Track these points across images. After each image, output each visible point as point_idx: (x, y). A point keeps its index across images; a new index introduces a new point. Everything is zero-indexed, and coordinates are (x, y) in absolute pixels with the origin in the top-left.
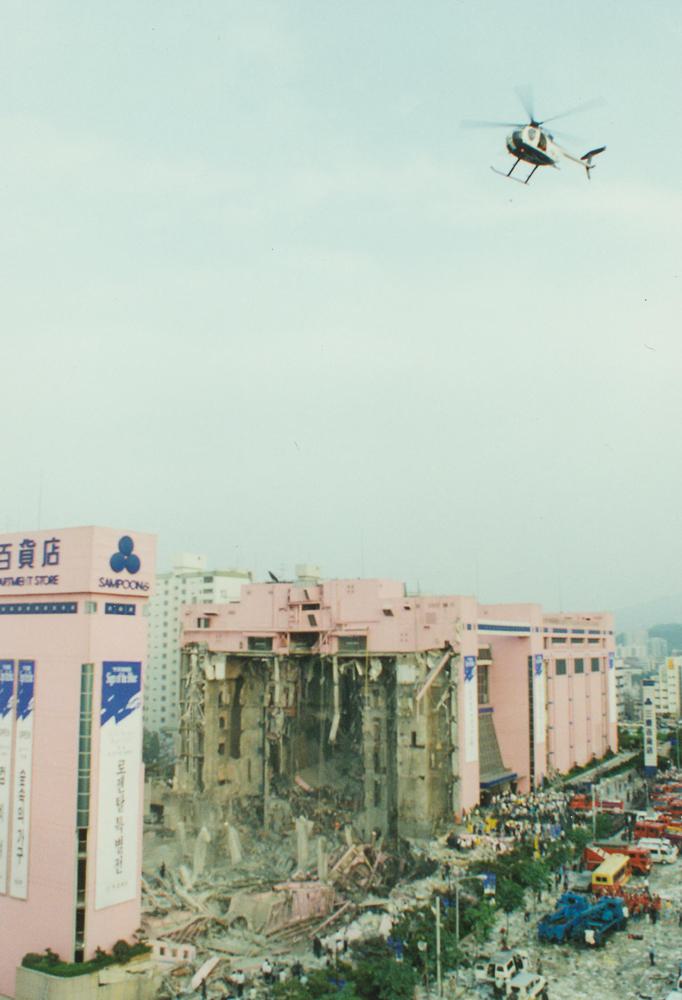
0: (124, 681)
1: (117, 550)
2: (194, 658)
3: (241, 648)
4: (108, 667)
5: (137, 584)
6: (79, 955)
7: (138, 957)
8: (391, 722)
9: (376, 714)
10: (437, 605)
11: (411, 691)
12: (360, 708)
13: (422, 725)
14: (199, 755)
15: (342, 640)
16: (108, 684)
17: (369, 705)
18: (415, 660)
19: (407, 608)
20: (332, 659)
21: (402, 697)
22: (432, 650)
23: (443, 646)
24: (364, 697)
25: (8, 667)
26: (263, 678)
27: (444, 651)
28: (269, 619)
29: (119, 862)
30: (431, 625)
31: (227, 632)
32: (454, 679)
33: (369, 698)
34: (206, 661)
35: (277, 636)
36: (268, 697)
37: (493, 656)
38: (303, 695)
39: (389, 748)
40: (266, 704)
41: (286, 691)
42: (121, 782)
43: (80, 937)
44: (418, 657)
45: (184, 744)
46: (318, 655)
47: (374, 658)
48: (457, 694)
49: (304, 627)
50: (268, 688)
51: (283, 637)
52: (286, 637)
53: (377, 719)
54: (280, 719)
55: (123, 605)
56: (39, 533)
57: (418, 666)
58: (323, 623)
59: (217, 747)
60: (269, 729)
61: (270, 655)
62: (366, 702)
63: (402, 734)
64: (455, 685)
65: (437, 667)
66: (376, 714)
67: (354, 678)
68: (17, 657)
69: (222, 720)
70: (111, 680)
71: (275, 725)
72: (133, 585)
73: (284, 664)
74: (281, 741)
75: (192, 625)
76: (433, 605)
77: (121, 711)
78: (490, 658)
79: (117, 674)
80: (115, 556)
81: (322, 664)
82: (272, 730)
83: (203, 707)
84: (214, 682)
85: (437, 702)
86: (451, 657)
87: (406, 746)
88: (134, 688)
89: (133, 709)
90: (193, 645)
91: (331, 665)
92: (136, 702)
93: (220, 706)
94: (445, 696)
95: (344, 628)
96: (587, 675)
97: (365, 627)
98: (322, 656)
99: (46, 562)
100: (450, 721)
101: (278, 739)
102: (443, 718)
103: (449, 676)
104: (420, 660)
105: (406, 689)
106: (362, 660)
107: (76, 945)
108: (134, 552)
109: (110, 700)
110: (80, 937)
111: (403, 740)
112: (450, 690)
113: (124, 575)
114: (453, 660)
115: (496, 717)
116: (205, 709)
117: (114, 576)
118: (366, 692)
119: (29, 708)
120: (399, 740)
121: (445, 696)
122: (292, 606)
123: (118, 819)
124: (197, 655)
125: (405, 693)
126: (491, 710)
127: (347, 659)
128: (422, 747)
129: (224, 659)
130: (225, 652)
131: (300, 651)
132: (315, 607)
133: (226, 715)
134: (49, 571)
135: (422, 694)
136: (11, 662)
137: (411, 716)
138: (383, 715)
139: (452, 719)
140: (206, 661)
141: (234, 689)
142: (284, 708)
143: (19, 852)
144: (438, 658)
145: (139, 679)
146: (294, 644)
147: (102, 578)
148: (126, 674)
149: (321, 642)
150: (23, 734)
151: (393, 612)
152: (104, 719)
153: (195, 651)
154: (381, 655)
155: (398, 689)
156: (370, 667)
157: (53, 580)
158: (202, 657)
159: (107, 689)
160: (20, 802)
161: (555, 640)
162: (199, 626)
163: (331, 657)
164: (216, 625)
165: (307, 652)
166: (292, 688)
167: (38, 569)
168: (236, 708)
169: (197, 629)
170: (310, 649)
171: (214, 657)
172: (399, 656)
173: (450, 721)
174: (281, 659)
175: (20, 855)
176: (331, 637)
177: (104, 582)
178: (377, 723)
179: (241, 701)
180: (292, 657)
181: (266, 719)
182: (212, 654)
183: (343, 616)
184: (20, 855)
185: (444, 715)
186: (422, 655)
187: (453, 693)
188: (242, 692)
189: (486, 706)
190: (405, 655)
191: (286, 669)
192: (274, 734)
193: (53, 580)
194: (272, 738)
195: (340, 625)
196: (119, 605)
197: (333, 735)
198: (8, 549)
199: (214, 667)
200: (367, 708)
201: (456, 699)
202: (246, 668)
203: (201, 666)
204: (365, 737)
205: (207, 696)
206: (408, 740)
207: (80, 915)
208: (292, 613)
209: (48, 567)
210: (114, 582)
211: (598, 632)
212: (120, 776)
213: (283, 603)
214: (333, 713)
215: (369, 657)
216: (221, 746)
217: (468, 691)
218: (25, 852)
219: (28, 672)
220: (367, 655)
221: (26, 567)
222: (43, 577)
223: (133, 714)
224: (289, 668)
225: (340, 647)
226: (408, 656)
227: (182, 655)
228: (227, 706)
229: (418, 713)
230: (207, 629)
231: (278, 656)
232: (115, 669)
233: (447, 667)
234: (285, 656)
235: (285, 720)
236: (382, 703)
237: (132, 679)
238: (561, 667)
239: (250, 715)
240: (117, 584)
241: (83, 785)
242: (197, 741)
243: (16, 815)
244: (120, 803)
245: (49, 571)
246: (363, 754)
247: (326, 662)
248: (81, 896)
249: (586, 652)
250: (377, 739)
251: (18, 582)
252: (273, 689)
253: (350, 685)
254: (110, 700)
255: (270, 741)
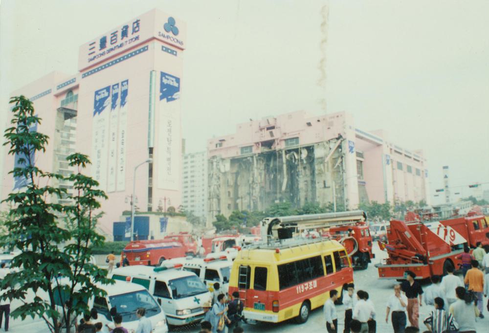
0: (171, 83)
1: (167, 22)
2: (215, 164)
3: (237, 153)
4: (163, 75)
5: (177, 41)
6: (150, 209)
7: (180, 217)
8: (313, 182)
9: (306, 179)
10: (334, 117)
11: (322, 160)
12: (297, 177)
13: (329, 177)
14: (218, 209)
15: (285, 140)
16: (163, 83)
17: (302, 175)
18: (324, 145)
19: (319, 121)
20: (282, 152)
21: (318, 164)
22: (332, 139)
23: (337, 136)
24: (299, 171)
25: (116, 87)
26: (249, 170)
27: (338, 139)
28: (252, 137)
29: (169, 169)
30: (331, 128)
31: (230, 147)
32: (344, 151)
33: (301, 171)
34: (221, 163)
35: (255, 145)
36: (251, 179)
37: (365, 155)
38: (270, 189)
39: (312, 194)
40: (250, 182)
41: (260, 174)
42: (170, 131)
43: (150, 201)
44: (325, 143)
45: (211, 205)
46: (275, 150)
47: (303, 148)
48: (345, 158)
49: (267, 137)
50: (251, 175)
51: (258, 145)
52: (259, 145)
53: (306, 181)
54: (257, 189)
55: (171, 50)
56: (129, 20)
57: (325, 148)
58: (277, 134)
59: (227, 205)
60: (252, 194)
61: (252, 155)
62: (300, 173)
63: (318, 183)
64: (344, 154)
65: (334, 146)
66: (306, 179)
67: (294, 162)
68: (120, 82)
69: (229, 192)
70: (165, 81)
71: (255, 192)
72: (176, 41)
73: (259, 161)
74: (258, 200)
75: (213, 147)
76: (332, 118)
77: (170, 97)
78: (363, 157)
79: (168, 79)
80: (166, 24)
81: (277, 153)
82: (254, 195)
83: (220, 186)
84: (225, 173)
85: (335, 164)
86: (342, 141)
87: (321, 188)
88: (177, 89)
89: (176, 99)
90: (214, 157)
91: (282, 154)
92: (178, 96)
93: (228, 186)
94: (339, 160)
95: (287, 135)
96: (414, 175)
97: (298, 133)
98: (277, 150)
99: (134, 31)
100: (343, 173)
101: (257, 198)
102: (339, 170)
103: (341, 151)
104: (326, 145)
105: (320, 160)
106: (297, 151)
107: (148, 205)
108: (176, 25)
109: (164, 90)
110: (150, 201)
111: (319, 186)
112: (342, 157)
113: (171, 34)
114: (343, 142)
115: (368, 188)
116: (221, 186)
117: (166, 34)
118: (300, 168)
119: (126, 101)
120: (317, 185)
121: (339, 160)
122: (261, 130)
123: (168, 148)
124: (216, 162)
125: (319, 162)
126: (364, 183)
127: (289, 151)
128: (329, 187)
129: (229, 161)
130: (229, 158)
131: (266, 150)
132: (273, 128)
133: (231, 190)
134: (135, 35)
135: (327, 159)
136: (118, 84)
137: (323, 173)
138: (309, 179)
139: (343, 171)
140: (221, 163)
141: (234, 179)
142: (259, 183)
143: (121, 169)
144: (335, 143)
145: (179, 85)
146: (263, 147)
147: (160, 32)
148: (172, 81)
149: (276, 143)
150: (123, 114)
151: (312, 123)
152: (162, 98)
153: (215, 160)
154: (306, 146)
155: (315, 161)
156: (301, 153)
157: (137, 38)
158: (218, 163)
159: (163, 85)
160: (122, 146)
161: (396, 151)
162: (217, 146)
163: (281, 150)
164: (225, 145)
165: (270, 150)
166: (263, 172)
167: (130, 35)
168: (236, 186)
169: (216, 149)
170: (270, 148)
171: (224, 161)
172: (315, 145)
173: (343, 173)
174: (257, 155)
175: (122, 170)
176: (281, 140)
177: (161, 34)
178: (306, 183)
179: (239, 183)
180: (261, 155)
181: (251, 190)
182: (223, 159)
183: (286, 129)
184: (122, 170)
185: (340, 172)
186: (327, 143)
187: (343, 158)
188: (239, 179)
189: (360, 180)
190: (318, 143)
191: (260, 164)
192: (255, 196)
193: (137, 38)
194: (254, 198)
195: (285, 134)
196: (168, 49)
197: (284, 188)
198: (116, 34)
199: (225, 166)
200: (301, 176)
201: (345, 161)
202: (240, 166)
203: (218, 167)
204: (300, 191)
205: (221, 180)
206: (322, 185)
207: (150, 190)
208: (261, 132)
209: (134, 33)
210: (166, 36)
211: (419, 157)
212: (169, 128)
213: (257, 129)
214: (283, 178)
215: (301, 148)
216: (229, 205)
217: (351, 160)
218: (124, 169)
219: (125, 85)
220: (299, 147)
221: (125, 38)
222: (132, 39)
223: (176, 100)
224: (261, 163)
225: (287, 144)
226: (320, 144)
227: (209, 163)
228: (232, 186)
229: (326, 171)
230: (221, 148)
231: (255, 154)
232: (167, 77)
233: (340, 147)
234: (259, 154)
235: (260, 190)
236: (308, 172)
237: (176, 85)
238: (400, 166)
239: (243, 191)
240: (168, 37)
241: (150, 99)
242: (217, 204)
243: (120, 151)
244: (169, 141)
245: (135, 35)
246: (300, 199)
247: (279, 153)
248: (150, 181)
249: (415, 165)
250: (306, 191)
251: (121, 45)
252: (253, 174)
253: (292, 167)
254: (164, 90)
255: (253, 200)
